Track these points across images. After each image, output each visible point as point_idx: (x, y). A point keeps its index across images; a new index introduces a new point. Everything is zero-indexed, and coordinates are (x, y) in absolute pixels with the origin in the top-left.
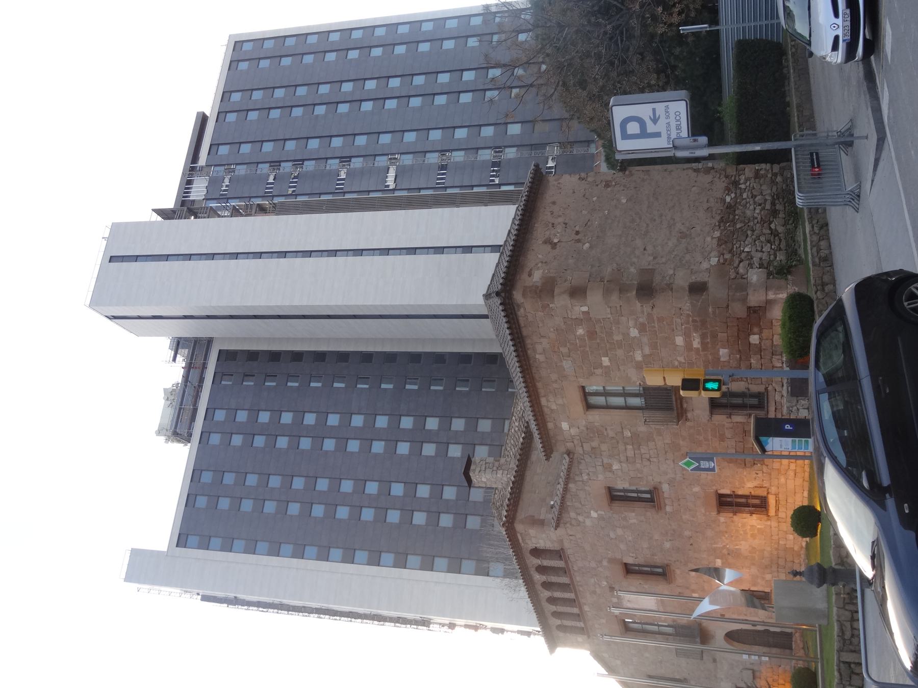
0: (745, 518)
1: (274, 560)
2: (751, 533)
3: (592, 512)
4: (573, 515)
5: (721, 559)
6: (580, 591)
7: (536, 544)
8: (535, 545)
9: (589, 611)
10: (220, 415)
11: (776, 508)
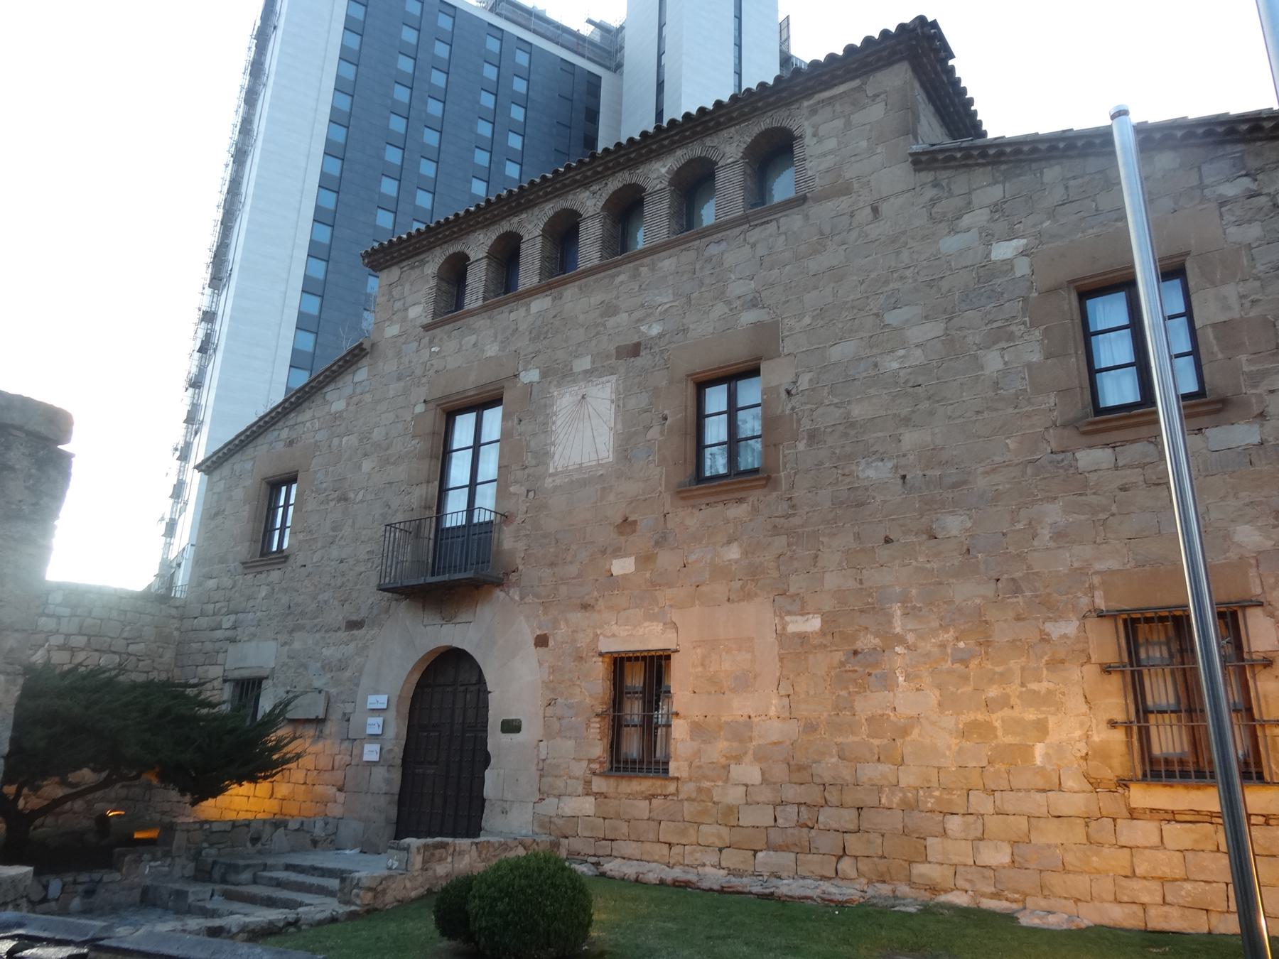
0: (1087, 702)
1: (330, 83)
2: (997, 724)
3: (1019, 243)
4: (996, 193)
5: (823, 633)
6: (613, 277)
7: (814, 135)
8: (809, 131)
9: (528, 310)
10: (522, 59)
11: (1181, 812)
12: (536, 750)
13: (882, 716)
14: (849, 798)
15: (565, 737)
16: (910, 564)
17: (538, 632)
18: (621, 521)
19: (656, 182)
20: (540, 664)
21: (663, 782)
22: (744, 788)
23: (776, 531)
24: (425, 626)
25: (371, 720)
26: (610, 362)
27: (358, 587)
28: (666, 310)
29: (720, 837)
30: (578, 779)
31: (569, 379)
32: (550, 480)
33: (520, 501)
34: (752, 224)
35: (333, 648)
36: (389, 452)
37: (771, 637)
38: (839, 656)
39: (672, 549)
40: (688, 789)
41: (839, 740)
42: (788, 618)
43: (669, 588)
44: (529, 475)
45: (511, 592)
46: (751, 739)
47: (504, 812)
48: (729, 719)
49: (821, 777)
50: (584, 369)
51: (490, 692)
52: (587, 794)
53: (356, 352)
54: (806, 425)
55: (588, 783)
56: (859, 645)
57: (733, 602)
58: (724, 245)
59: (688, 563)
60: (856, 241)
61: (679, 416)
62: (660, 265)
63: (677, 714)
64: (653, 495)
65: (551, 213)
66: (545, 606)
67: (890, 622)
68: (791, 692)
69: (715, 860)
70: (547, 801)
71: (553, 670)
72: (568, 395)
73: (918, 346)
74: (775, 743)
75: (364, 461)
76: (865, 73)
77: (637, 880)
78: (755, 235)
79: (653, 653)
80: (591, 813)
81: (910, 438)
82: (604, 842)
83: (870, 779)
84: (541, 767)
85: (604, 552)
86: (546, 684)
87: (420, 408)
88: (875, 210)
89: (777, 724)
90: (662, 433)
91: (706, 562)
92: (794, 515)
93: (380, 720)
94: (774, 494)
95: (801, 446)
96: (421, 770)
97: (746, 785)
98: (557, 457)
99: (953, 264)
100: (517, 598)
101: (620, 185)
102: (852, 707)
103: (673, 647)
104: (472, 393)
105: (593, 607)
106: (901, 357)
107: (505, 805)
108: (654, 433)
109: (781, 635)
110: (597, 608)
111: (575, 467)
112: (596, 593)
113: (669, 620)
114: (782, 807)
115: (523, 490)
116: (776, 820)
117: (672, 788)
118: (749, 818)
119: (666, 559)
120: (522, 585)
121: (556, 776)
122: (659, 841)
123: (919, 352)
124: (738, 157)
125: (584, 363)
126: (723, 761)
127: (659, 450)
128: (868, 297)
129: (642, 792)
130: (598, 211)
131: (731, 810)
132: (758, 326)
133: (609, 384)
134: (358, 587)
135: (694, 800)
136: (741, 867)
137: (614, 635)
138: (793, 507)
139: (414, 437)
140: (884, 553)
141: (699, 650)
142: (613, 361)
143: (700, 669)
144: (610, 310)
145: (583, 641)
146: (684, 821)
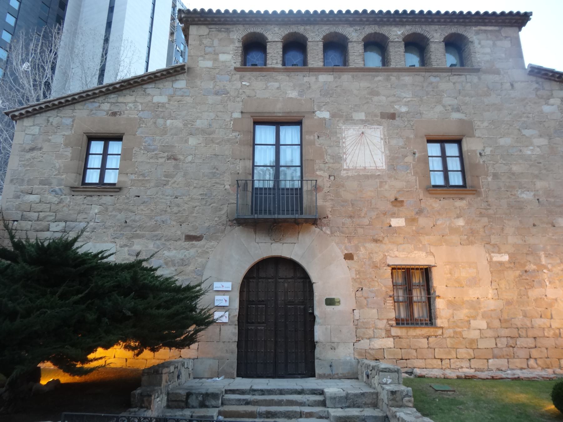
5: (510, 262)
7: (479, 43)
12: (352, 315)
13: (541, 298)
14: (530, 333)
15: (371, 308)
16: (546, 236)
17: (346, 252)
18: (393, 200)
19: (395, 37)
20: (350, 269)
21: (435, 329)
22: (479, 331)
23: (481, 215)
24: (258, 243)
25: (217, 297)
26: (377, 119)
27: (194, 215)
28: (409, 101)
29: (469, 354)
30: (381, 329)
31: (350, 122)
32: (345, 172)
33: (325, 180)
34: (452, 73)
35: (174, 251)
36: (211, 136)
37: (486, 263)
38: (518, 273)
39: (427, 217)
40: (449, 332)
41: (523, 309)
42: (492, 254)
43: (427, 235)
44: (329, 167)
45: (324, 229)
46: (480, 308)
47: (333, 348)
48: (468, 299)
49: (516, 325)
50: (361, 118)
51: (314, 283)
52: (388, 337)
53: (179, 69)
54: (491, 170)
55: (388, 332)
56: (527, 268)
57: (464, 245)
58: (438, 79)
59: (436, 225)
60: (505, 96)
61: (423, 154)
62: (402, 78)
63: (439, 297)
64: (412, 189)
65: (328, 32)
66: (350, 239)
67: (540, 259)
68: (498, 287)
69: (468, 365)
70: (362, 341)
71: (358, 272)
72: (352, 130)
73: (538, 147)
74: (492, 310)
75: (190, 138)
76: (501, 26)
77: (444, 378)
78: (455, 78)
79: (409, 267)
80: (392, 346)
81: (540, 184)
82: (402, 361)
83: (539, 325)
84: (356, 322)
85: (385, 214)
86: (354, 280)
87: (237, 115)
88: (512, 85)
89: (492, 302)
90: (414, 160)
91: (446, 225)
92: (490, 209)
93: (227, 297)
94: (479, 199)
95: (490, 179)
96: (253, 327)
97: (480, 330)
98: (348, 161)
99: (549, 117)
100: (328, 232)
101: (373, 32)
102: (527, 294)
103: (433, 264)
104: (280, 115)
105: (381, 241)
106: (531, 150)
107: (333, 345)
108: (409, 159)
109: (490, 262)
110: (384, 242)
111: (361, 168)
112: (382, 234)
113: (428, 251)
114: (499, 339)
115: (326, 175)
116: (496, 344)
117: (440, 332)
118: (482, 344)
119: (422, 221)
120: (331, 225)
121: (366, 328)
122: (435, 358)
123: (538, 149)
124: (441, 41)
125: (362, 116)
126: (467, 319)
127: (413, 168)
128: (513, 121)
129: (423, 335)
130: (360, 40)
131: (473, 342)
132: (461, 121)
133: (379, 130)
134: (194, 215)
135: (453, 337)
136: (482, 367)
137: (396, 257)
138: (489, 205)
139: (234, 131)
140: (534, 230)
141: (448, 267)
142: (379, 119)
143: (449, 275)
144: (374, 93)
145: (377, 258)
146: (448, 348)
